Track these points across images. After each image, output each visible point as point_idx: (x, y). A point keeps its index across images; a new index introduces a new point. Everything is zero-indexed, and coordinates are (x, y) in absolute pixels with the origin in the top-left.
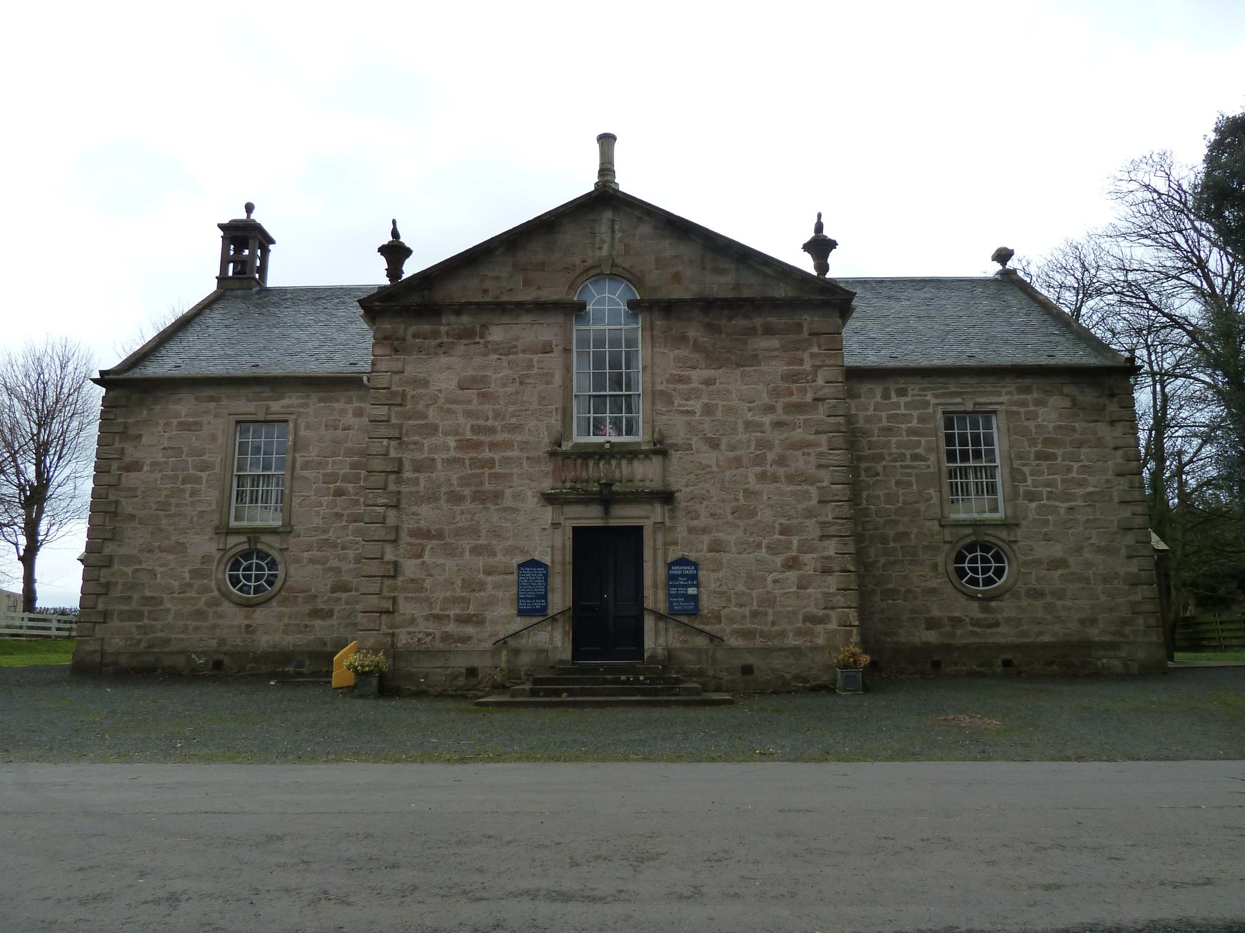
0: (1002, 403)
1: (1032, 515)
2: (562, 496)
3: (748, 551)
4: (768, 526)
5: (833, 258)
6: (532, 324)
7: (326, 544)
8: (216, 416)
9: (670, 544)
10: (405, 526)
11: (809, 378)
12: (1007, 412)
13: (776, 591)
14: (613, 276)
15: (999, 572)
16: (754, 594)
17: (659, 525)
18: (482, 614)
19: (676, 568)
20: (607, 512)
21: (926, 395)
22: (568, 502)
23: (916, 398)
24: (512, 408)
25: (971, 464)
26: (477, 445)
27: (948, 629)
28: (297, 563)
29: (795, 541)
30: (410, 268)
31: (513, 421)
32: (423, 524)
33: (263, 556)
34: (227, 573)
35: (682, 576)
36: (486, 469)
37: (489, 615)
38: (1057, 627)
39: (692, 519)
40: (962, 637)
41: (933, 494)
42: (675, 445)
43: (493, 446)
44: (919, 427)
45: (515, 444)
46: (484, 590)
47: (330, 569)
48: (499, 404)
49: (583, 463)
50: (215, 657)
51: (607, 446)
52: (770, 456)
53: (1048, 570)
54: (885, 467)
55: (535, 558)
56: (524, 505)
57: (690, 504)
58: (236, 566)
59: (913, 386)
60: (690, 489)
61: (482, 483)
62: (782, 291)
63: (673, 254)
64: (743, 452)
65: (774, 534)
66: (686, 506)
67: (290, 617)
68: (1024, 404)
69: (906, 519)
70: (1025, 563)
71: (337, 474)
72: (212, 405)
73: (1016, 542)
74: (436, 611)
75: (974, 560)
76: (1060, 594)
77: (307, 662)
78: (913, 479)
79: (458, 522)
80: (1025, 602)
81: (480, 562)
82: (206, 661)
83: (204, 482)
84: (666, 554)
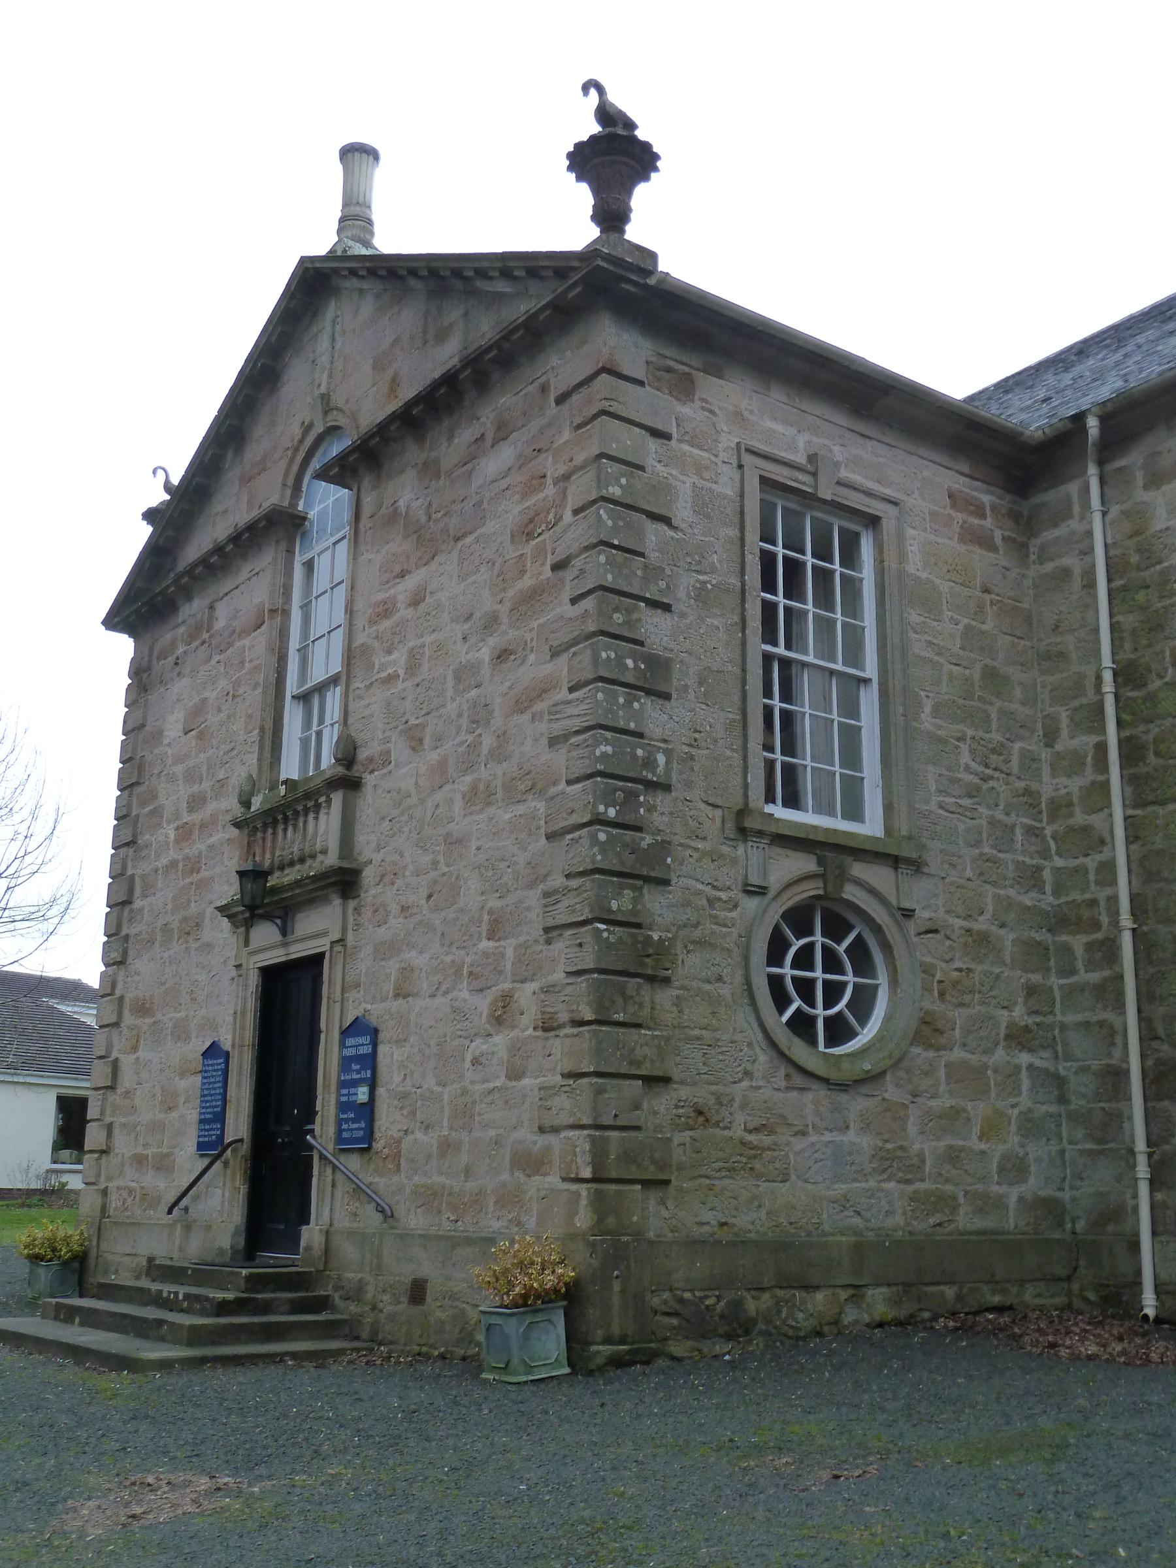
3: (444, 987)
10: (129, 996)
65: (480, 939)
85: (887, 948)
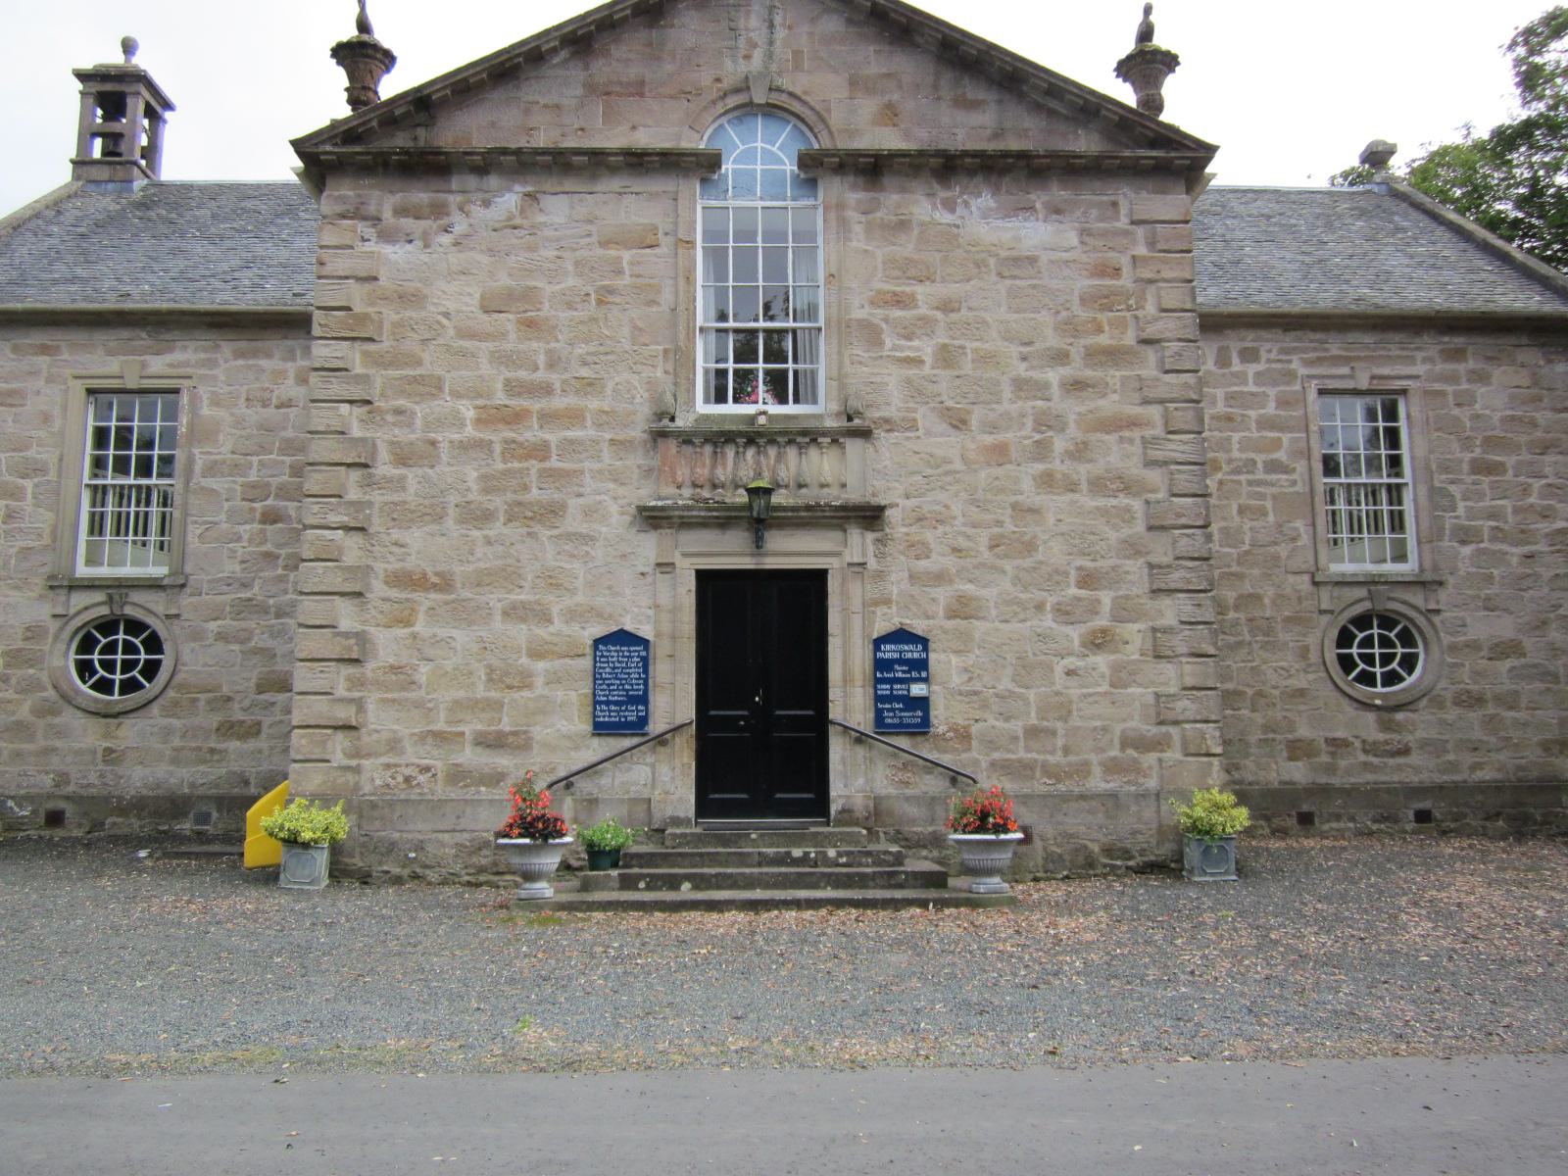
0: (1417, 377)
1: (1463, 568)
2: (677, 513)
4: (1057, 572)
5: (1172, 89)
6: (620, 194)
7: (248, 607)
8: (50, 380)
9: (876, 603)
11: (1131, 302)
12: (1427, 393)
13: (1072, 691)
14: (772, 111)
15: (1409, 663)
16: (1031, 695)
17: (856, 569)
18: (525, 732)
19: (888, 647)
20: (758, 542)
21: (1290, 361)
22: (686, 524)
23: (1274, 366)
24: (581, 350)
25: (1363, 479)
26: (517, 418)
27: (1325, 758)
28: (195, 640)
29: (1106, 598)
30: (390, 87)
31: (585, 372)
32: (412, 563)
33: (135, 627)
34: (73, 656)
35: (901, 661)
36: (534, 462)
37: (538, 732)
38: (1502, 757)
39: (918, 558)
40: (1350, 771)
41: (1302, 529)
42: (887, 421)
43: (548, 418)
44: (1279, 416)
45: (588, 416)
46: (529, 686)
47: (256, 651)
48: (558, 341)
49: (715, 453)
50: (51, 805)
51: (762, 420)
52: (1060, 444)
53: (1490, 659)
54: (1221, 483)
55: (628, 627)
56: (604, 529)
57: (913, 529)
58: (87, 644)
59: (1268, 346)
60: (914, 502)
61: (526, 488)
62: (1085, 143)
63: (884, 70)
64: (1010, 435)
65: (1069, 586)
66: (907, 534)
67: (184, 736)
68: (1452, 379)
69: (1256, 572)
70: (1453, 648)
71: (268, 485)
72: (43, 361)
73: (1438, 611)
74: (440, 725)
75: (1367, 642)
76: (1510, 701)
77: (215, 815)
78: (1269, 504)
79: (479, 560)
80: (1452, 714)
81: (520, 633)
82: (34, 812)
83: (29, 496)
84: (868, 622)
85: (1421, 632)
